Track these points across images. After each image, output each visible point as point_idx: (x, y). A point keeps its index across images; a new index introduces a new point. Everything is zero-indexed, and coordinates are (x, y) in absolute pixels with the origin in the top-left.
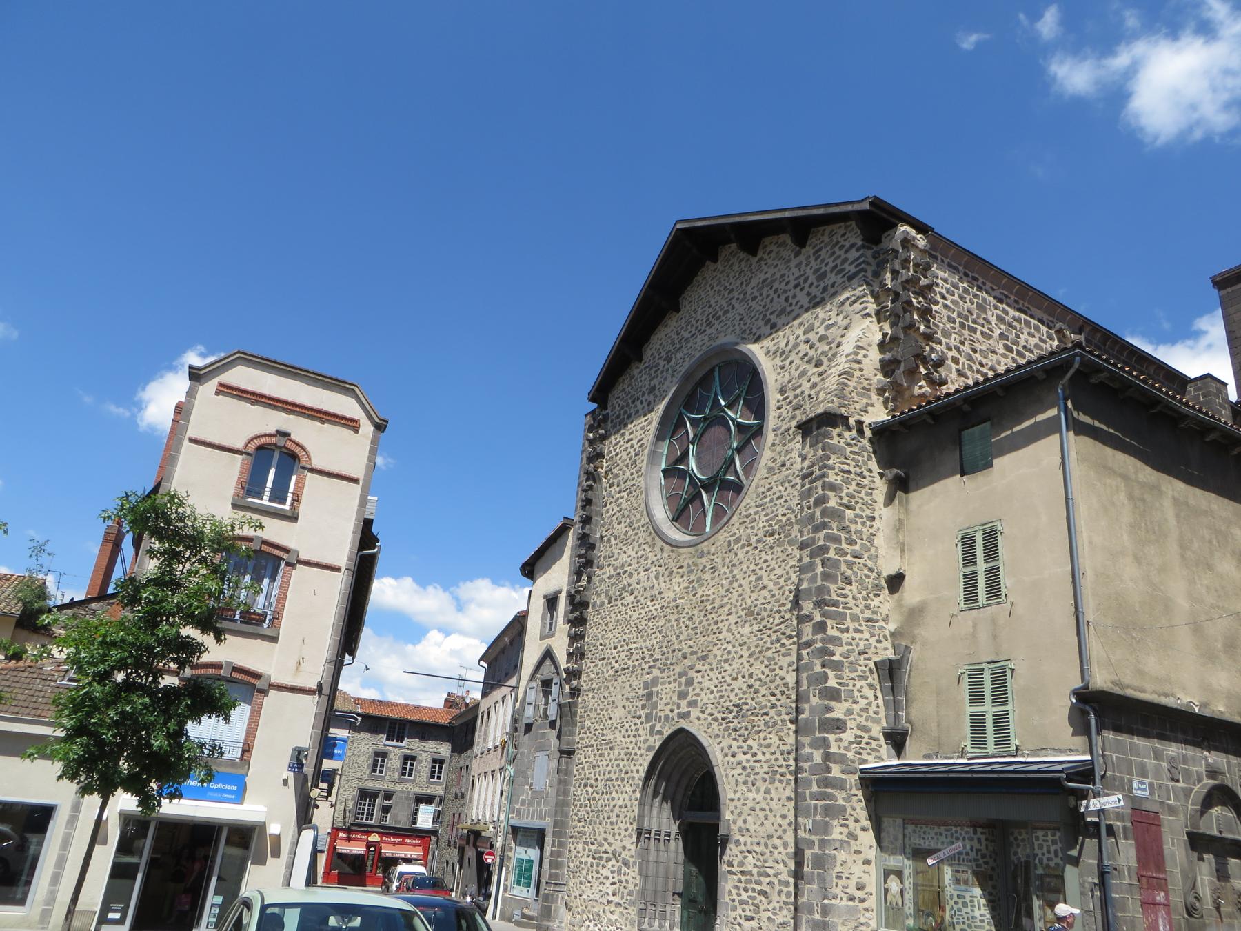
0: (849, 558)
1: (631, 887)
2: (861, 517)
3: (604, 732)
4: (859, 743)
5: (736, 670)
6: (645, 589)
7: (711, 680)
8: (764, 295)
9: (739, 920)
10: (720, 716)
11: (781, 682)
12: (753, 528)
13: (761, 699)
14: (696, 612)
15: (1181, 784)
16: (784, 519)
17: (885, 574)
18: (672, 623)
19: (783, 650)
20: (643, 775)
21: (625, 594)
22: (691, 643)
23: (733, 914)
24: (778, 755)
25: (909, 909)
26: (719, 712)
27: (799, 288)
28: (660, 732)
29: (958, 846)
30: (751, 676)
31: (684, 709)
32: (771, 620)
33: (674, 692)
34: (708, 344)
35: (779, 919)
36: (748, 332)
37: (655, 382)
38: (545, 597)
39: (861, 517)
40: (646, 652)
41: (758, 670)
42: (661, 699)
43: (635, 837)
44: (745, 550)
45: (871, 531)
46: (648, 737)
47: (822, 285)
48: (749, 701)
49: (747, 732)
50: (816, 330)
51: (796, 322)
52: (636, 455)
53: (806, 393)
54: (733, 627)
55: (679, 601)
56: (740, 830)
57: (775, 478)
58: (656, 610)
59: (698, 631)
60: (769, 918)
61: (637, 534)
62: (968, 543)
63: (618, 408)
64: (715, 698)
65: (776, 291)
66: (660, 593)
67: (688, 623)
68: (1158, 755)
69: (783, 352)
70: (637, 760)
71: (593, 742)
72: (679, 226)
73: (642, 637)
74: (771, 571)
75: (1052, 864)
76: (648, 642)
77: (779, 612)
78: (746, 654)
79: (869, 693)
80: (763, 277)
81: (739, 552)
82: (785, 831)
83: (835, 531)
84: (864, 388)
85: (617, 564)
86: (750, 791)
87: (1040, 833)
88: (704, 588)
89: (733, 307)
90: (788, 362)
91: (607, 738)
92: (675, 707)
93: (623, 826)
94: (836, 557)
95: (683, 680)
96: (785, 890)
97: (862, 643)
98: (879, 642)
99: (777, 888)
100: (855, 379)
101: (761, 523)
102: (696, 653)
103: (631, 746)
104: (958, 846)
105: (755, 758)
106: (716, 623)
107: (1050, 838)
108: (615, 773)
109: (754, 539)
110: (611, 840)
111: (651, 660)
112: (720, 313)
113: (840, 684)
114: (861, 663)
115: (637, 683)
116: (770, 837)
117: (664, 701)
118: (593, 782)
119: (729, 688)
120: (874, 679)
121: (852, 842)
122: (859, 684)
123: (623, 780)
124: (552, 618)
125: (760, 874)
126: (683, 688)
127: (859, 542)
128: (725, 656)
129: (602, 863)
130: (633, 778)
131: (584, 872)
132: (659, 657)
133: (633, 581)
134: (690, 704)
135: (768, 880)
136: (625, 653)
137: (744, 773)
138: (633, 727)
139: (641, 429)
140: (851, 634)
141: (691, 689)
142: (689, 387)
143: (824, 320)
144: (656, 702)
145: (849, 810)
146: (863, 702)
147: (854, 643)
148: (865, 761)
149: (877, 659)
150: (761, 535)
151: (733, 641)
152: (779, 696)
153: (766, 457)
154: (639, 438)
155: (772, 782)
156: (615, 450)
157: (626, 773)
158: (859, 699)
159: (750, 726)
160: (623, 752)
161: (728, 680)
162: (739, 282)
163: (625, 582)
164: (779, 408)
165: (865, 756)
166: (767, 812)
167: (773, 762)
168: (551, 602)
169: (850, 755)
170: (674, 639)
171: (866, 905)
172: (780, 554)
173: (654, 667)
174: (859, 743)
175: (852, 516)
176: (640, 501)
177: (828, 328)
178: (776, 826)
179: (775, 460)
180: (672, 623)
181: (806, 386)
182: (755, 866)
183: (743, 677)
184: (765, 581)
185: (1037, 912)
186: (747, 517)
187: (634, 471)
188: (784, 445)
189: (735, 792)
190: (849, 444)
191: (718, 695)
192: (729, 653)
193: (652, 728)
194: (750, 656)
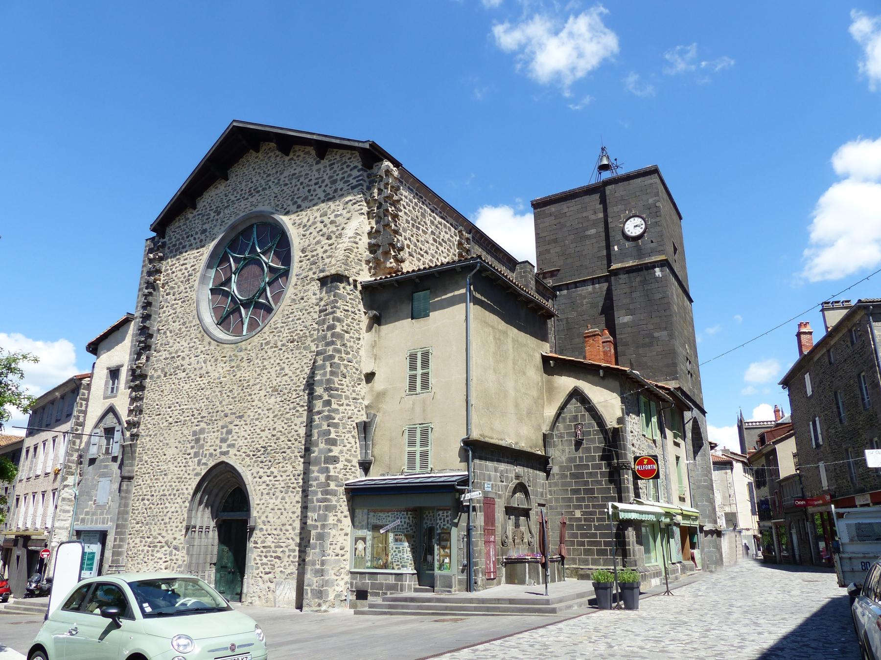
0: (345, 362)
1: (180, 562)
2: (353, 338)
3: (159, 464)
4: (346, 469)
5: (264, 425)
6: (195, 369)
7: (246, 431)
8: (293, 184)
9: (261, 575)
10: (251, 453)
12: (279, 336)
13: (282, 443)
14: (235, 387)
15: (504, 483)
16: (301, 333)
17: (364, 372)
18: (217, 393)
19: (297, 414)
20: (192, 492)
22: (231, 407)
23: (257, 572)
24: (291, 477)
25: (368, 557)
26: (251, 451)
27: (318, 186)
28: (205, 464)
29: (398, 522)
30: (274, 429)
31: (224, 449)
32: (290, 395)
33: (217, 438)
34: (250, 208)
35: (288, 571)
36: (280, 206)
37: (206, 226)
38: (108, 368)
39: (353, 338)
40: (196, 411)
41: (280, 424)
42: (207, 442)
43: (184, 531)
45: (358, 346)
46: (196, 467)
47: (334, 188)
48: (273, 444)
49: (270, 463)
51: (315, 208)
52: (189, 275)
53: (320, 255)
54: (263, 398)
55: (222, 379)
56: (264, 522)
57: (297, 306)
58: (204, 384)
59: (237, 400)
60: (281, 571)
61: (189, 331)
62: (413, 358)
63: (174, 240)
64: (248, 442)
65: (302, 184)
66: (207, 373)
67: (229, 394)
68: (496, 470)
69: (305, 226)
70: (187, 482)
71: (149, 471)
72: (235, 124)
73: (192, 401)
75: (445, 527)
76: (197, 404)
77: (296, 390)
78: (271, 415)
79: (352, 440)
80: (293, 172)
81: (269, 351)
82: (294, 521)
83: (339, 347)
84: (359, 260)
85: (171, 350)
87: (441, 512)
88: (241, 372)
89: (270, 187)
90: (308, 232)
91: (162, 468)
92: (218, 448)
93: (175, 525)
94: (339, 362)
95: (224, 430)
96: (293, 554)
97: (350, 412)
98: (359, 411)
99: (287, 553)
100: (354, 254)
101: (285, 333)
102: (235, 413)
103: (182, 473)
104: (398, 522)
105: (276, 479)
106: (250, 395)
107: (445, 514)
108: (168, 490)
109: (279, 344)
110: (164, 533)
111: (199, 417)
112: (260, 189)
113: (337, 436)
114: (349, 423)
115: (187, 431)
116: (283, 525)
117: (209, 444)
118: (149, 497)
119: (259, 436)
120: (355, 433)
121: (339, 524)
122: (347, 435)
123: (175, 495)
124: (113, 384)
126: (224, 435)
127: (351, 353)
128: (257, 416)
129: (156, 549)
130: (183, 494)
131: (141, 557)
132: (207, 415)
133: (186, 362)
134: (229, 446)
135: (281, 549)
136: (178, 411)
137: (268, 488)
138: (184, 461)
139: (194, 258)
140: (345, 407)
141: (230, 436)
142: (233, 235)
143: (334, 210)
144: (203, 444)
145: (338, 507)
146: (349, 446)
147: (346, 412)
148: (348, 479)
149: (357, 421)
150: (285, 341)
151: (262, 407)
152: (293, 442)
153: (290, 292)
154: (192, 264)
156: (171, 269)
157: (178, 490)
158: (347, 444)
159: (272, 460)
160: (175, 477)
161: (258, 431)
162: (274, 171)
163: (178, 363)
164: (301, 262)
165: (348, 476)
166: (282, 511)
167: (288, 481)
168: (114, 373)
169: (341, 476)
170: (218, 403)
171: (344, 558)
172: (297, 355)
173: (201, 421)
174: (346, 469)
175: (348, 337)
176: (192, 309)
177: (336, 216)
178: (288, 518)
179: (296, 295)
180: (217, 393)
181: (320, 251)
182: (273, 542)
184: (287, 371)
185: (436, 552)
186: (275, 329)
187: (187, 286)
188: (304, 286)
189: (260, 500)
190: (348, 294)
191: (250, 441)
192: (259, 414)
193: (199, 462)
194: (274, 417)
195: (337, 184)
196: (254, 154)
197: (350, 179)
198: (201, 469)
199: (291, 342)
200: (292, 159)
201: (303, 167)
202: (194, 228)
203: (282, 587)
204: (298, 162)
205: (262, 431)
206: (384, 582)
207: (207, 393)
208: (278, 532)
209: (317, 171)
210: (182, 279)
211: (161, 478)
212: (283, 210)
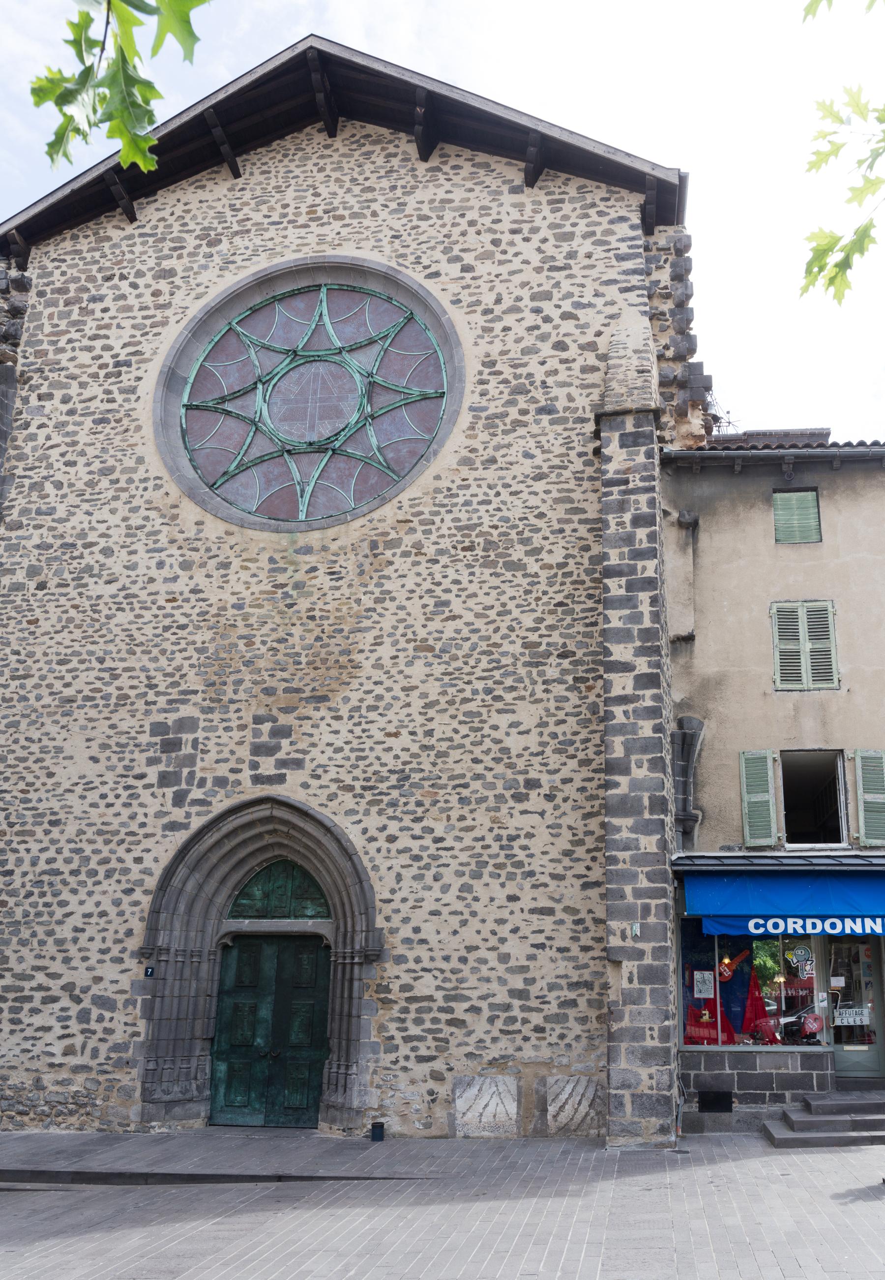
5: (396, 723)
7: (336, 732)
9: (402, 1063)
10: (358, 785)
11: (495, 748)
12: (427, 532)
16: (495, 533)
17: (672, 633)
19: (499, 705)
21: (87, 579)
23: (392, 1056)
26: (355, 779)
30: (429, 733)
31: (268, 767)
36: (411, 258)
44: (409, 560)
48: (427, 767)
49: (420, 810)
50: (555, 301)
54: (387, 662)
60: (469, 1055)
70: (139, 843)
74: (469, 596)
76: (163, 662)
78: (418, 704)
82: (503, 940)
86: (430, 888)
90: (498, 326)
93: (97, 945)
95: (266, 727)
102: (298, 691)
105: (440, 845)
112: (346, 213)
116: (470, 949)
117: (213, 756)
125: (447, 998)
126: (265, 738)
128: (370, 700)
130: (126, 871)
134: (282, 763)
135: (466, 1005)
137: (416, 864)
138: (125, 794)
141: (285, 743)
155: (477, 875)
159: (427, 802)
161: (379, 736)
163: (88, 560)
167: (478, 850)
173: (184, 702)
177: (578, 305)
178: (486, 934)
182: (438, 988)
183: (412, 733)
184: (457, 606)
189: (393, 891)
191: (353, 756)
192: (379, 698)
194: (428, 706)
195: (575, 244)
196: (321, 138)
197: (612, 239)
198: (188, 815)
199: (464, 549)
200: (438, 169)
201: (471, 190)
202: (132, 261)
203: (474, 1090)
204: (457, 179)
205: (389, 735)
206: (774, 1071)
207: (198, 638)
208: (454, 963)
209: (514, 205)
210: (94, 369)
211: (39, 831)
212: (419, 268)
